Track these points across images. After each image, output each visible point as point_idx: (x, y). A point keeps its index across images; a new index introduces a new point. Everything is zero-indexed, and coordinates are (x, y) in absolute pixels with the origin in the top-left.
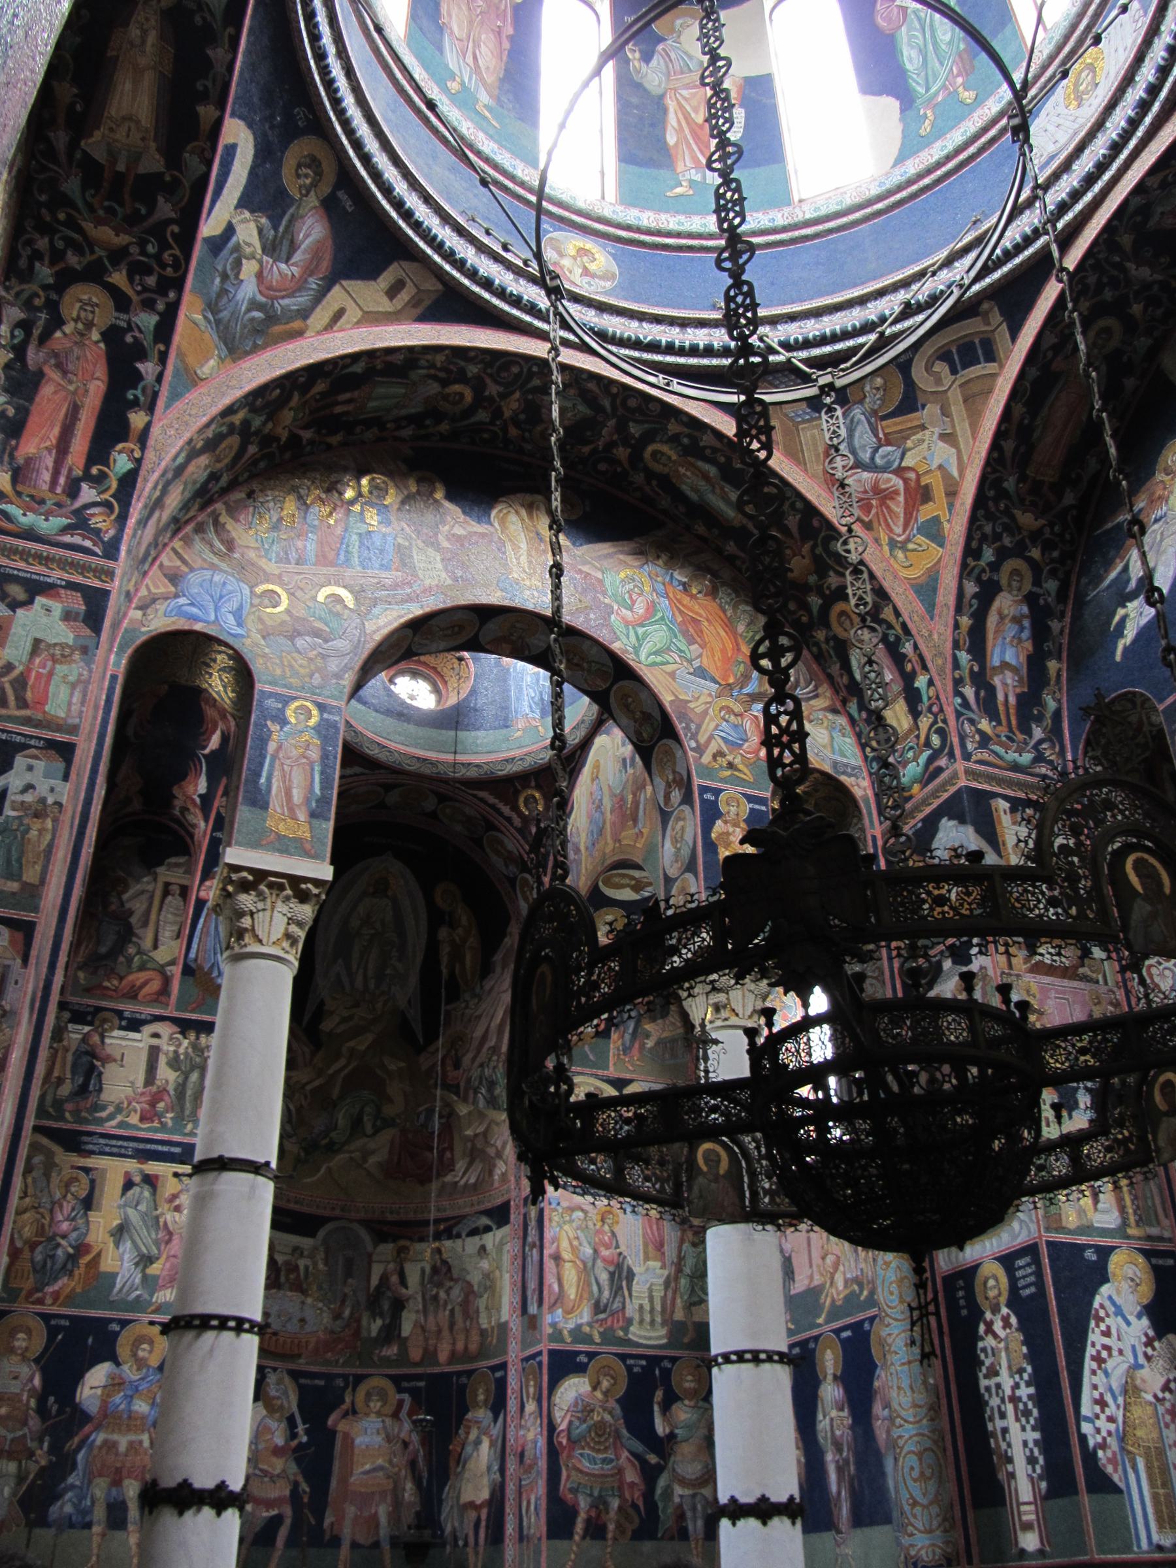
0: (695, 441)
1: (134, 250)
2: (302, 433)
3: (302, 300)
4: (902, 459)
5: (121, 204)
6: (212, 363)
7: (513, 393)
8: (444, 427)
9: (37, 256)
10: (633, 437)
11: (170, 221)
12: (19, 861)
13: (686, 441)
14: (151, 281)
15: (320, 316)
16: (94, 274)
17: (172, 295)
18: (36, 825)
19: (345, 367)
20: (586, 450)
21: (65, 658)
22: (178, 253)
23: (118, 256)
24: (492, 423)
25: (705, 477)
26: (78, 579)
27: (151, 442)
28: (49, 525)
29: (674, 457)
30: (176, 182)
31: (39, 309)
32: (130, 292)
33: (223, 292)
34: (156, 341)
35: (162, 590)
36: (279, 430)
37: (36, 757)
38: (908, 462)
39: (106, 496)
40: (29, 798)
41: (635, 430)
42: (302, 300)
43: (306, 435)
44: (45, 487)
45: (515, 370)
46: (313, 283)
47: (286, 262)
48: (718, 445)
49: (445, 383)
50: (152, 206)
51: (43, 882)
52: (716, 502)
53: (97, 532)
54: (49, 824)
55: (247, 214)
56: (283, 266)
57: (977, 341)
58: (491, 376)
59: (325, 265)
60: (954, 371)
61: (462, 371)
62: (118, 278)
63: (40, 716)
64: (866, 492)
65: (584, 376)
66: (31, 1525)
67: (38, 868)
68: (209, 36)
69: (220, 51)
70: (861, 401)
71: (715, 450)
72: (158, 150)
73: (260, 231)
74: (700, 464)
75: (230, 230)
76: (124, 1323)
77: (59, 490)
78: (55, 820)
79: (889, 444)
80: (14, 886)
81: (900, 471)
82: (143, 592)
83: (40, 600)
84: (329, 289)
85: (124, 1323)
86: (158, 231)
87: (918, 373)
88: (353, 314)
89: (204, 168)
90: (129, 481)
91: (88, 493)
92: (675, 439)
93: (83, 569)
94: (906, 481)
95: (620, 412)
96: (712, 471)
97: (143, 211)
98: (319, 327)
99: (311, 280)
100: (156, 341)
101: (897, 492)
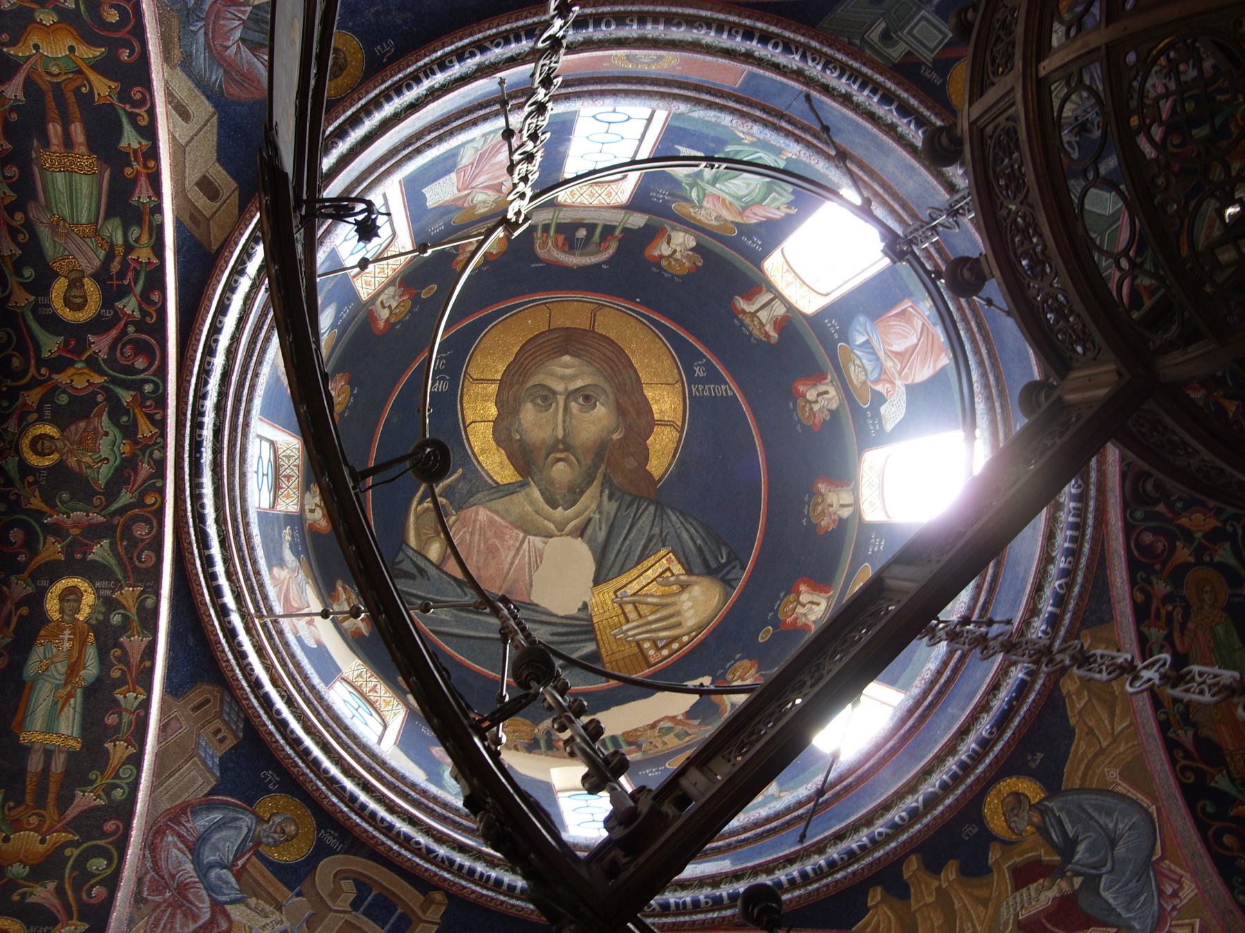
0: (125, 627)
2: (19, 80)
3: (201, 59)
4: (232, 902)
7: (101, 372)
10: (85, 554)
13: (116, 619)
19: (133, 118)
20: (37, 503)
24: (41, 362)
25: (74, 668)
29: (81, 617)
38: (235, 912)
41: (100, 551)
42: (201, 59)
45: (140, 363)
46: (217, 76)
47: (242, 39)
48: (135, 658)
49: (101, 276)
52: (42, 699)
56: (237, 35)
57: (399, 911)
58: (124, 332)
59: (235, 91)
60: (355, 905)
61: (124, 292)
64: (173, 877)
65: (157, 455)
70: (260, 820)
71: (124, 658)
74: (91, 653)
79: (238, 875)
81: (218, 908)
87: (327, 867)
92: (110, 604)
94: (213, 920)
95: (119, 520)
99: (221, 72)
101: (195, 918)
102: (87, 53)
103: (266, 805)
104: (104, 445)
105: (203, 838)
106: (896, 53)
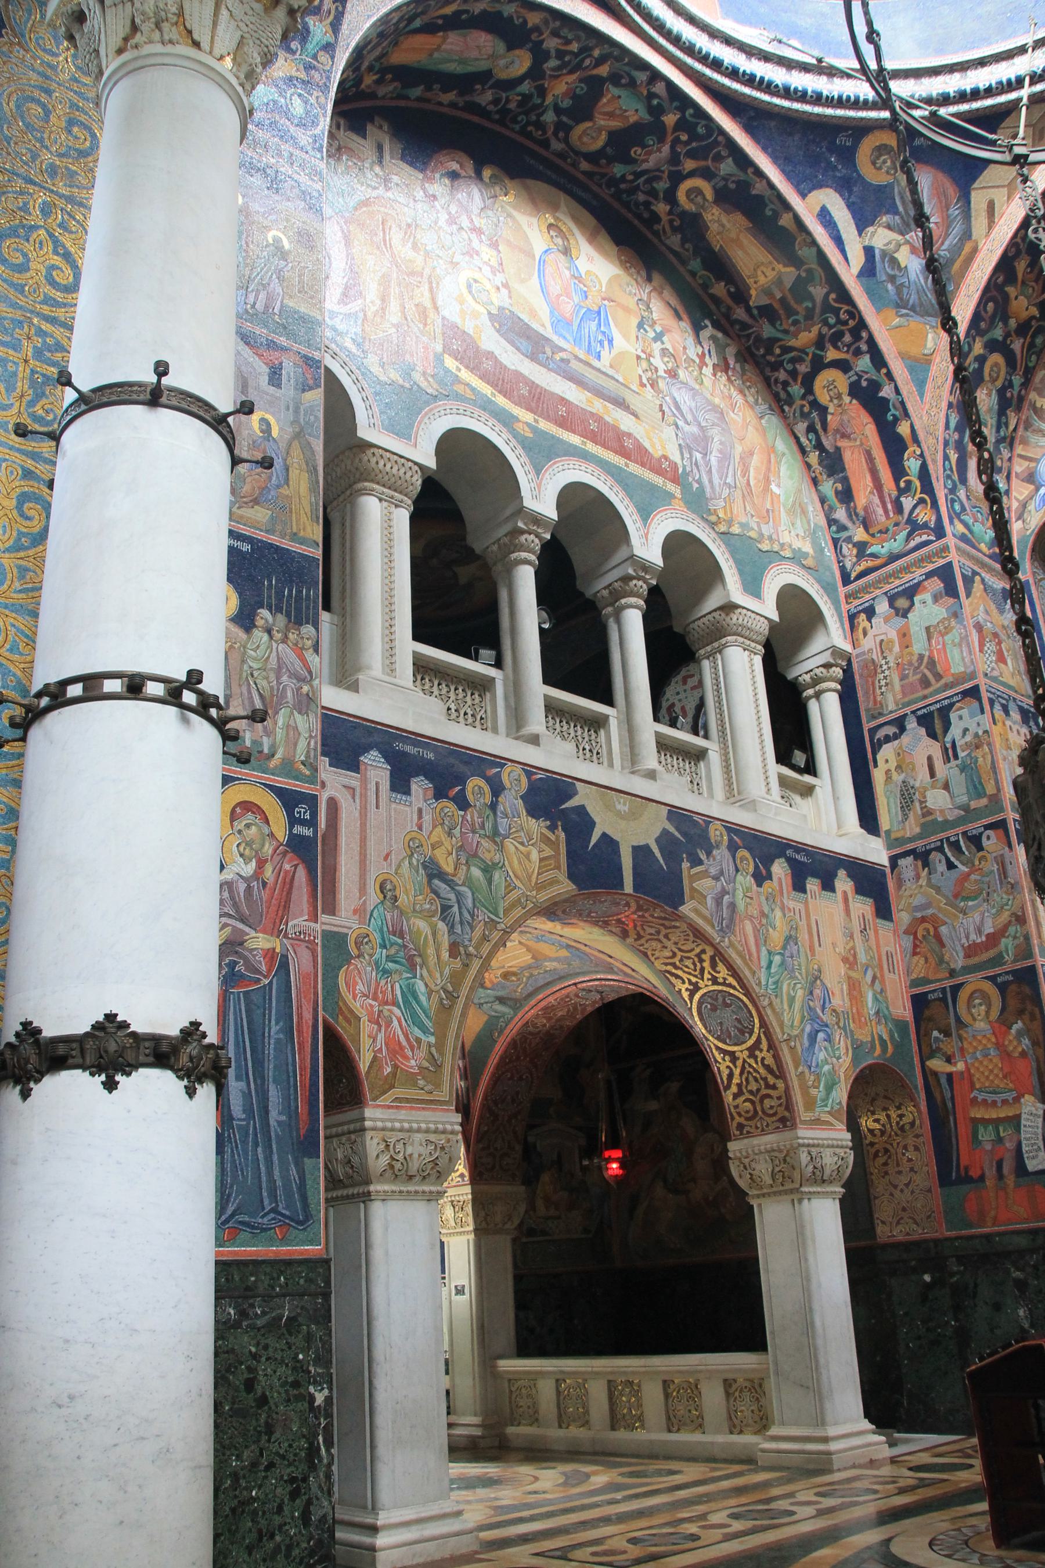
1: (825, 330)
5: (797, 313)
6: (930, 336)
9: (785, 384)
11: (827, 295)
12: (981, 783)
14: (847, 338)
15: (979, 223)
16: (819, 365)
17: (864, 334)
18: (978, 754)
21: (948, 630)
22: (846, 308)
23: (820, 343)
26: (930, 567)
27: (921, 435)
28: (895, 545)
30: (809, 271)
31: (810, 413)
32: (843, 356)
33: (899, 289)
34: (879, 371)
35: (1026, 493)
36: (1024, 315)
37: (961, 708)
39: (918, 496)
40: (968, 738)
42: (957, 229)
44: (883, 519)
46: (954, 211)
50: (811, 298)
51: (998, 790)
53: (925, 526)
54: (986, 747)
55: (871, 229)
59: (952, 191)
62: (832, 354)
63: (951, 679)
67: (992, 782)
68: (744, 186)
69: (757, 185)
72: (785, 266)
73: (889, 227)
75: (869, 251)
77: (891, 514)
78: (989, 744)
80: (984, 801)
82: (1015, 505)
83: (916, 599)
84: (969, 203)
86: (827, 308)
89: (814, 250)
90: (924, 474)
91: (908, 503)
93: (929, 558)
97: (810, 305)
98: (984, 232)
99: (951, 211)
100: (879, 371)
102: (1011, 290)
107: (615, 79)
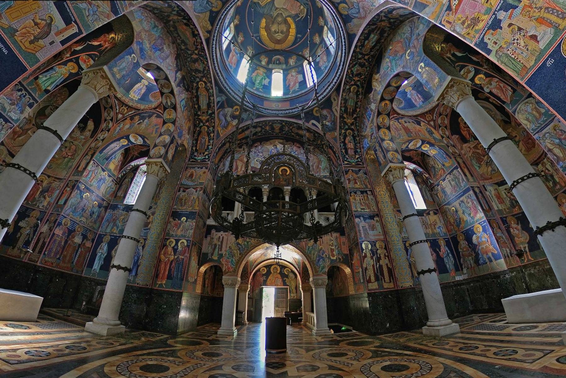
0: (360, 46)
8: (360, 90)
15: (336, 113)
41: (360, 56)
43: (355, 116)
49: (350, 92)
52: (374, 40)
59: (329, 110)
61: (348, 89)
66: (478, 266)
68: (299, 126)
74: (366, 43)
76: (473, 227)
85: (473, 227)
88: (336, 107)
96: (366, 42)
103: (346, 13)
104: (356, 70)
105: (357, 13)
106: (248, 113)
107: (273, 123)
